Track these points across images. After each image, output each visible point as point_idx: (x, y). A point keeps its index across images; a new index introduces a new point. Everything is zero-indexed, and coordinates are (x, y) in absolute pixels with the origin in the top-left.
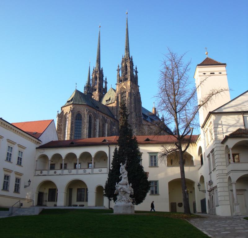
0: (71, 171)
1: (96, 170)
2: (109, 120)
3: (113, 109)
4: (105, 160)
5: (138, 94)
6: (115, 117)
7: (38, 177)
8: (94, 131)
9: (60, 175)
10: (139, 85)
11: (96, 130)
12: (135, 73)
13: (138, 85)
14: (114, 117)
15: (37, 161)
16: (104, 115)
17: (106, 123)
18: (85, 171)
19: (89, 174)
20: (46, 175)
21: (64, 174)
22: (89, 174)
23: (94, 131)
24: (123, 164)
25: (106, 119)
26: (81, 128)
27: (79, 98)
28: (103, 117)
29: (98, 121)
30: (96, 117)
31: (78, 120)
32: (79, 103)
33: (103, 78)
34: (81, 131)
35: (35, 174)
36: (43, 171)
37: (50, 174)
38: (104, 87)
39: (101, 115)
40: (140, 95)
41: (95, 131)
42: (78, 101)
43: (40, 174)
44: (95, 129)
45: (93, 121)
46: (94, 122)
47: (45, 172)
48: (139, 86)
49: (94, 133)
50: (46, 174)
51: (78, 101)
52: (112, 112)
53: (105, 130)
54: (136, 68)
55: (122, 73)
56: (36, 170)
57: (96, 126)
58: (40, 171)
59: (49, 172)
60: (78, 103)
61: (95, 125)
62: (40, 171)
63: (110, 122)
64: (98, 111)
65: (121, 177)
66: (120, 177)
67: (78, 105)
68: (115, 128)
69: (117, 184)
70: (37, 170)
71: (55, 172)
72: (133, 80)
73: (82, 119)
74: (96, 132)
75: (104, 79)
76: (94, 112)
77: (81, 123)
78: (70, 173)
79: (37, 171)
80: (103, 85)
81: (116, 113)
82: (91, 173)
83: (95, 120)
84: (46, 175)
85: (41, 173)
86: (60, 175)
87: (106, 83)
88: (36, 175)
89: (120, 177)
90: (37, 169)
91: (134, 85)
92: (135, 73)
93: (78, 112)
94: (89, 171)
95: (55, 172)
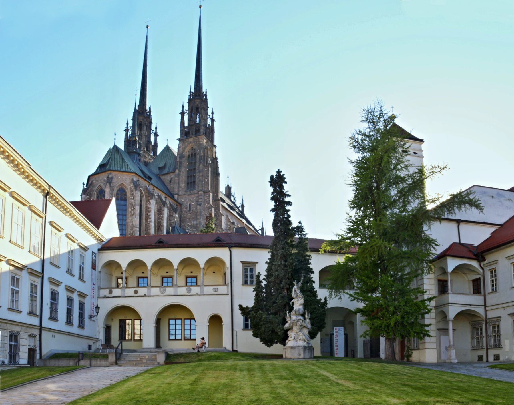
0: (165, 290)
1: (209, 290)
2: (168, 201)
3: (170, 182)
4: (214, 272)
5: (215, 160)
6: (176, 197)
7: (105, 300)
8: (146, 221)
9: (145, 296)
10: (216, 143)
11: (150, 218)
12: (209, 121)
13: (215, 144)
14: (173, 197)
15: (100, 272)
16: (160, 193)
17: (164, 206)
18: (189, 291)
19: (197, 294)
20: (119, 297)
21: (152, 295)
22: (197, 294)
23: (146, 221)
24: (297, 283)
25: (164, 199)
26: (125, 215)
27: (121, 160)
28: (158, 195)
29: (153, 202)
30: (151, 195)
31: (121, 200)
32: (122, 170)
33: (151, 125)
34: (126, 220)
35: (99, 295)
36: (113, 290)
37: (126, 295)
38: (153, 144)
39: (157, 192)
40: (217, 162)
41: (149, 220)
42: (119, 166)
43: (108, 295)
44: (148, 217)
45: (144, 202)
46: (146, 204)
47: (116, 292)
48: (215, 146)
49: (146, 225)
50: (120, 295)
51: (119, 166)
52: (168, 187)
53: (163, 220)
54: (213, 113)
55: (189, 120)
56: (100, 288)
57: (150, 212)
58: (108, 290)
59: (124, 291)
60: (119, 169)
61: (148, 211)
62: (108, 290)
63: (168, 205)
64: (152, 184)
65: (293, 303)
66: (291, 303)
67: (121, 173)
68: (177, 216)
69: (288, 314)
70: (101, 289)
71: (136, 292)
72: (208, 134)
73: (128, 199)
74: (150, 222)
75: (153, 127)
76: (146, 187)
77: (126, 205)
78: (162, 292)
79: (101, 291)
80: (150, 138)
81: (176, 190)
82: (199, 293)
83: (148, 201)
84: (119, 297)
85: (111, 292)
86: (145, 296)
87: (156, 135)
88: (101, 296)
89: (291, 303)
90: (102, 287)
91: (210, 143)
92: (209, 121)
93: (119, 185)
94: (195, 290)
95: (136, 292)
